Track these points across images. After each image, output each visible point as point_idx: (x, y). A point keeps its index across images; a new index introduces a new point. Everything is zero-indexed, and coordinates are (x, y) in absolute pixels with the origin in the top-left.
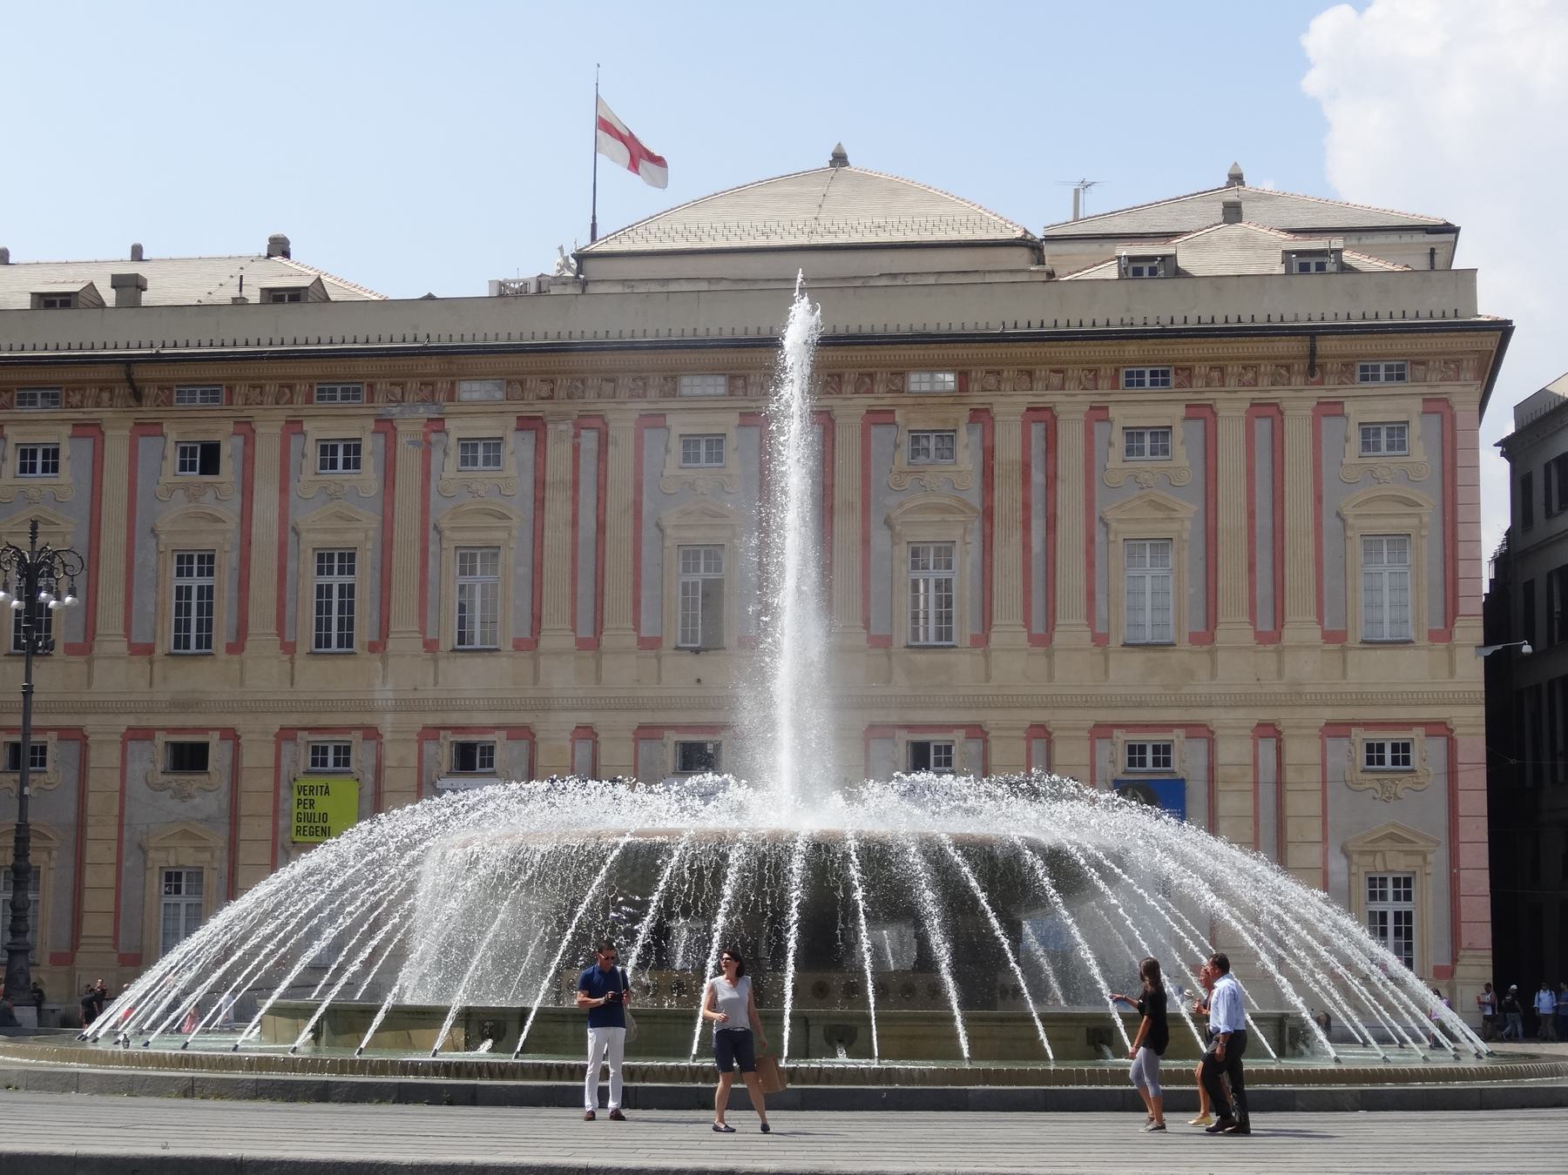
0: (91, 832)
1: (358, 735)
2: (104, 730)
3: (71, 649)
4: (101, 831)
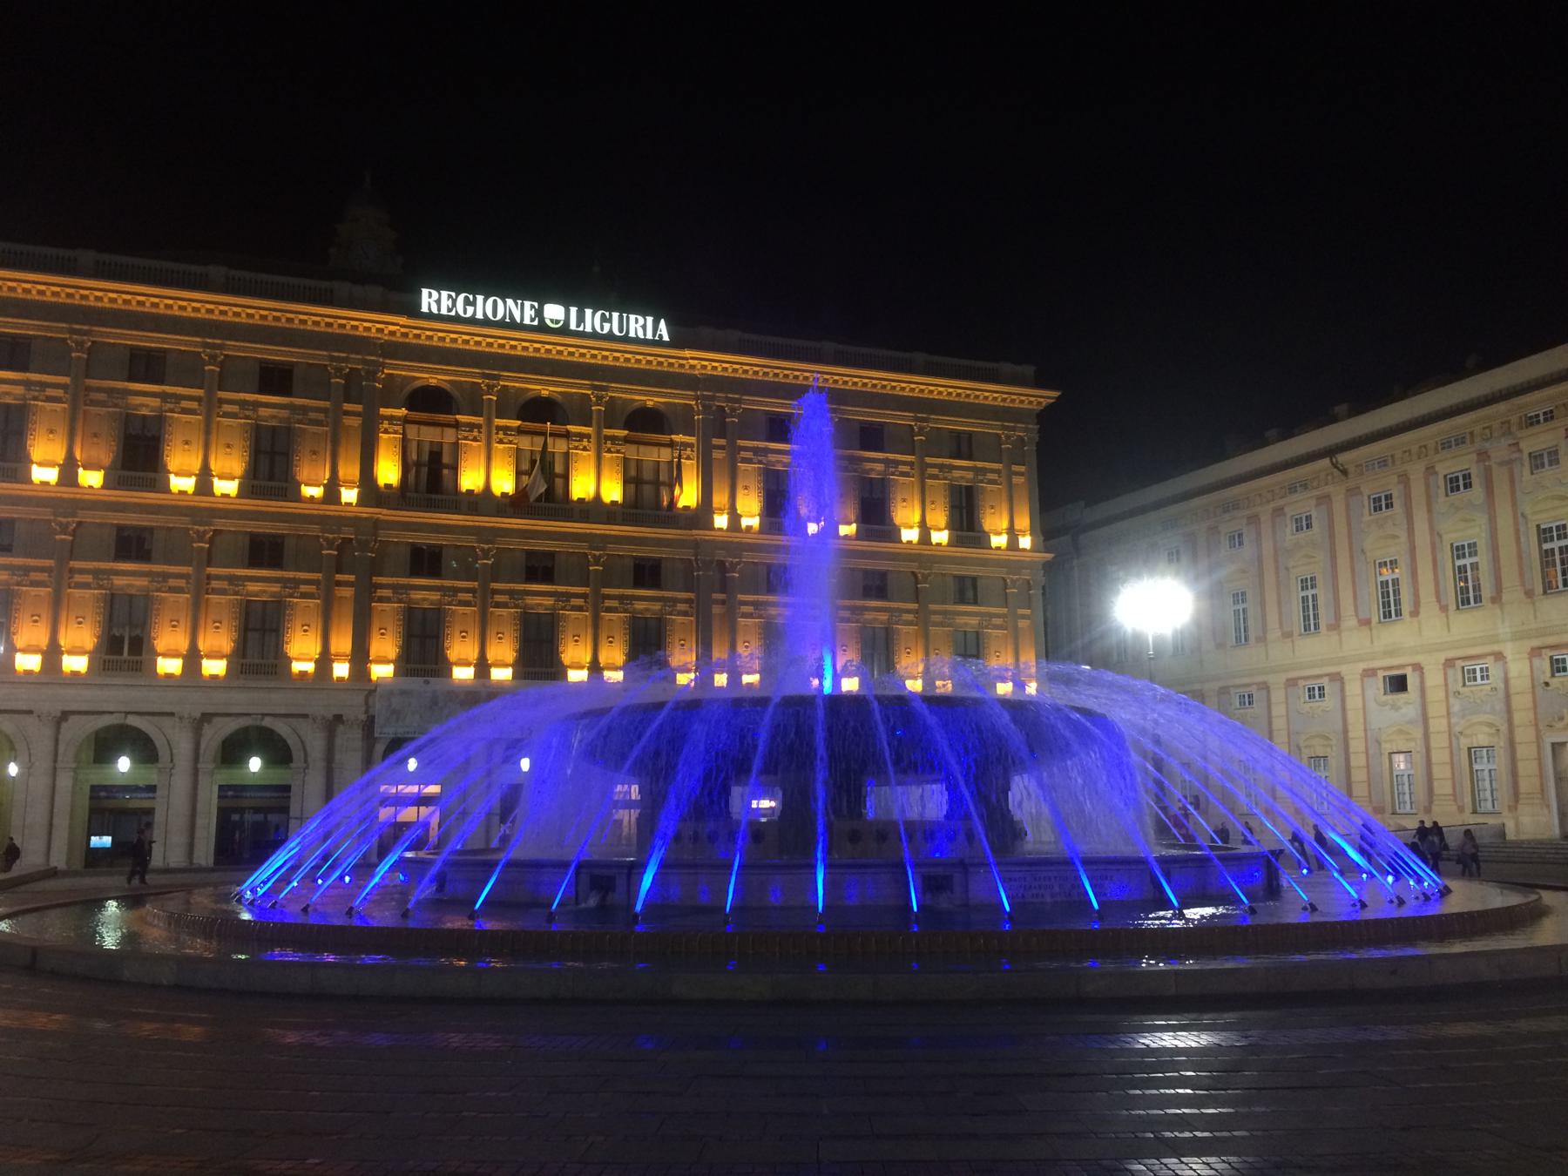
0: (1351, 735)
1: (1491, 658)
2: (1351, 672)
3: (1331, 628)
4: (1356, 732)
